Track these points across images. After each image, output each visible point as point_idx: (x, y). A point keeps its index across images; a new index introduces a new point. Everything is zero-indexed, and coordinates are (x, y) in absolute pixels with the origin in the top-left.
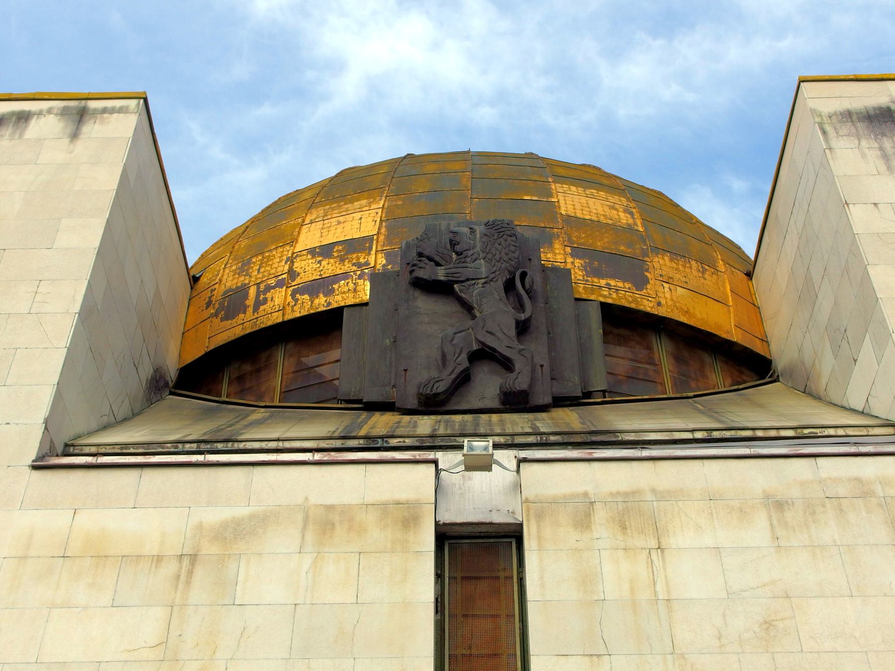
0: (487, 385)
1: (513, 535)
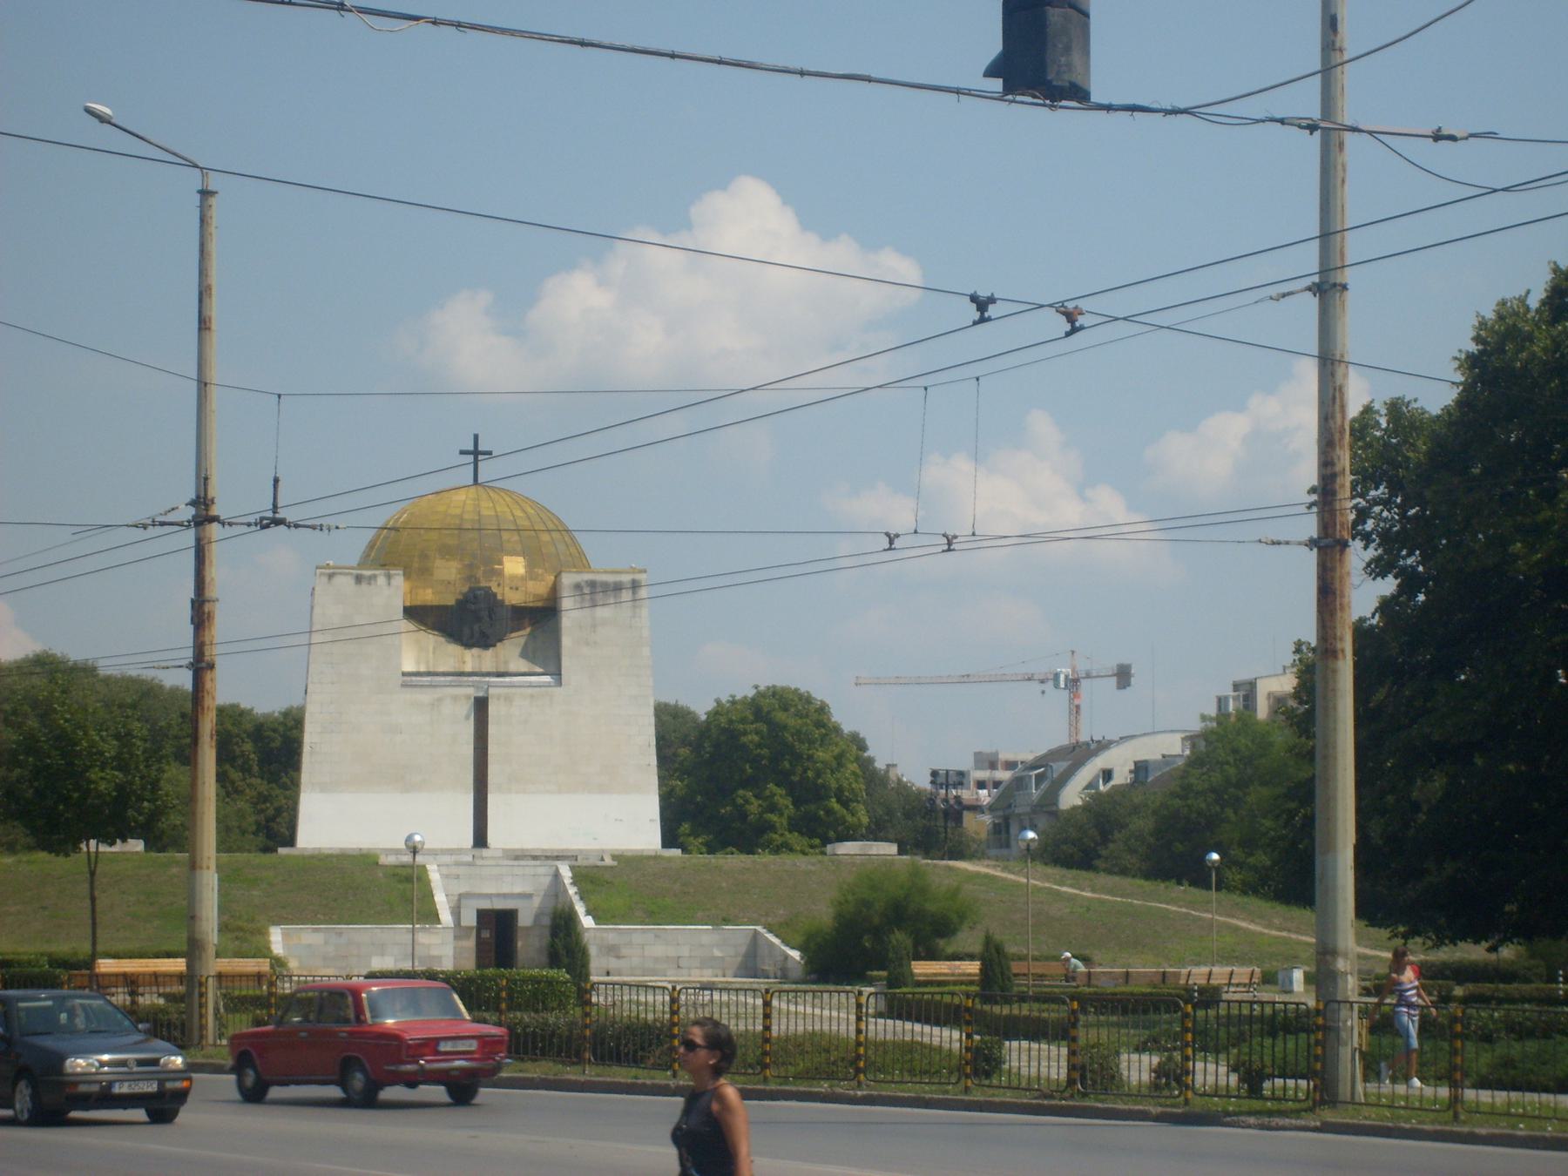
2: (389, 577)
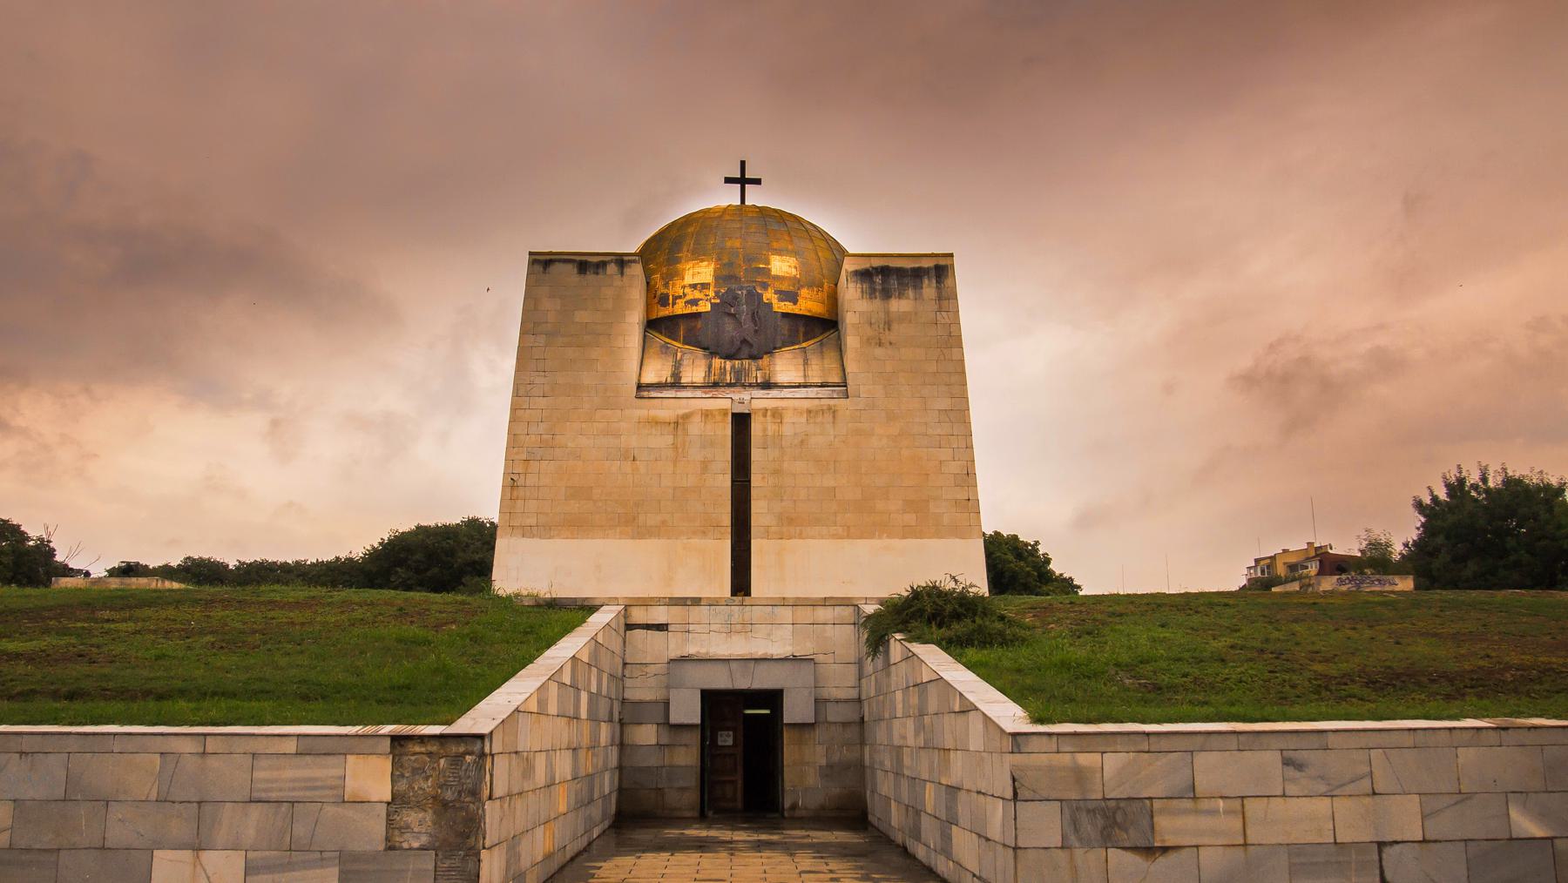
0: (746, 350)
1: (749, 415)
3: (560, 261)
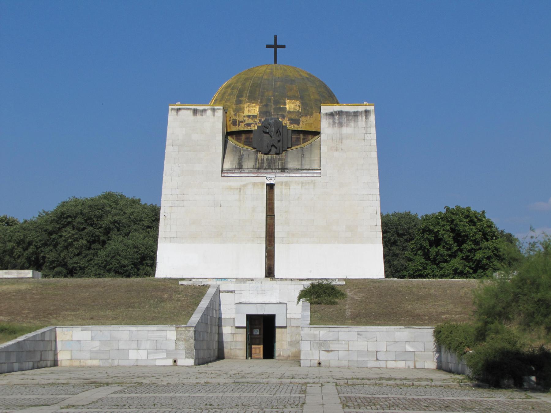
0: (274, 150)
1: (274, 184)
2: (214, 110)
3: (184, 109)
